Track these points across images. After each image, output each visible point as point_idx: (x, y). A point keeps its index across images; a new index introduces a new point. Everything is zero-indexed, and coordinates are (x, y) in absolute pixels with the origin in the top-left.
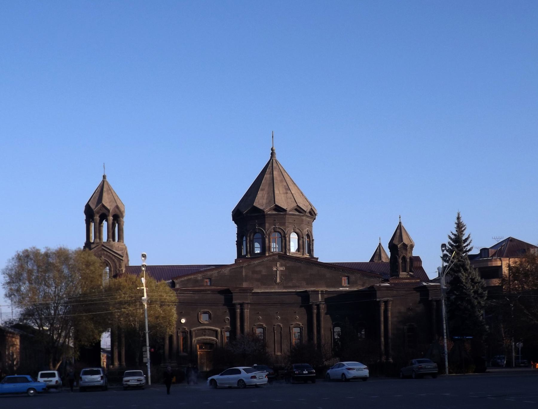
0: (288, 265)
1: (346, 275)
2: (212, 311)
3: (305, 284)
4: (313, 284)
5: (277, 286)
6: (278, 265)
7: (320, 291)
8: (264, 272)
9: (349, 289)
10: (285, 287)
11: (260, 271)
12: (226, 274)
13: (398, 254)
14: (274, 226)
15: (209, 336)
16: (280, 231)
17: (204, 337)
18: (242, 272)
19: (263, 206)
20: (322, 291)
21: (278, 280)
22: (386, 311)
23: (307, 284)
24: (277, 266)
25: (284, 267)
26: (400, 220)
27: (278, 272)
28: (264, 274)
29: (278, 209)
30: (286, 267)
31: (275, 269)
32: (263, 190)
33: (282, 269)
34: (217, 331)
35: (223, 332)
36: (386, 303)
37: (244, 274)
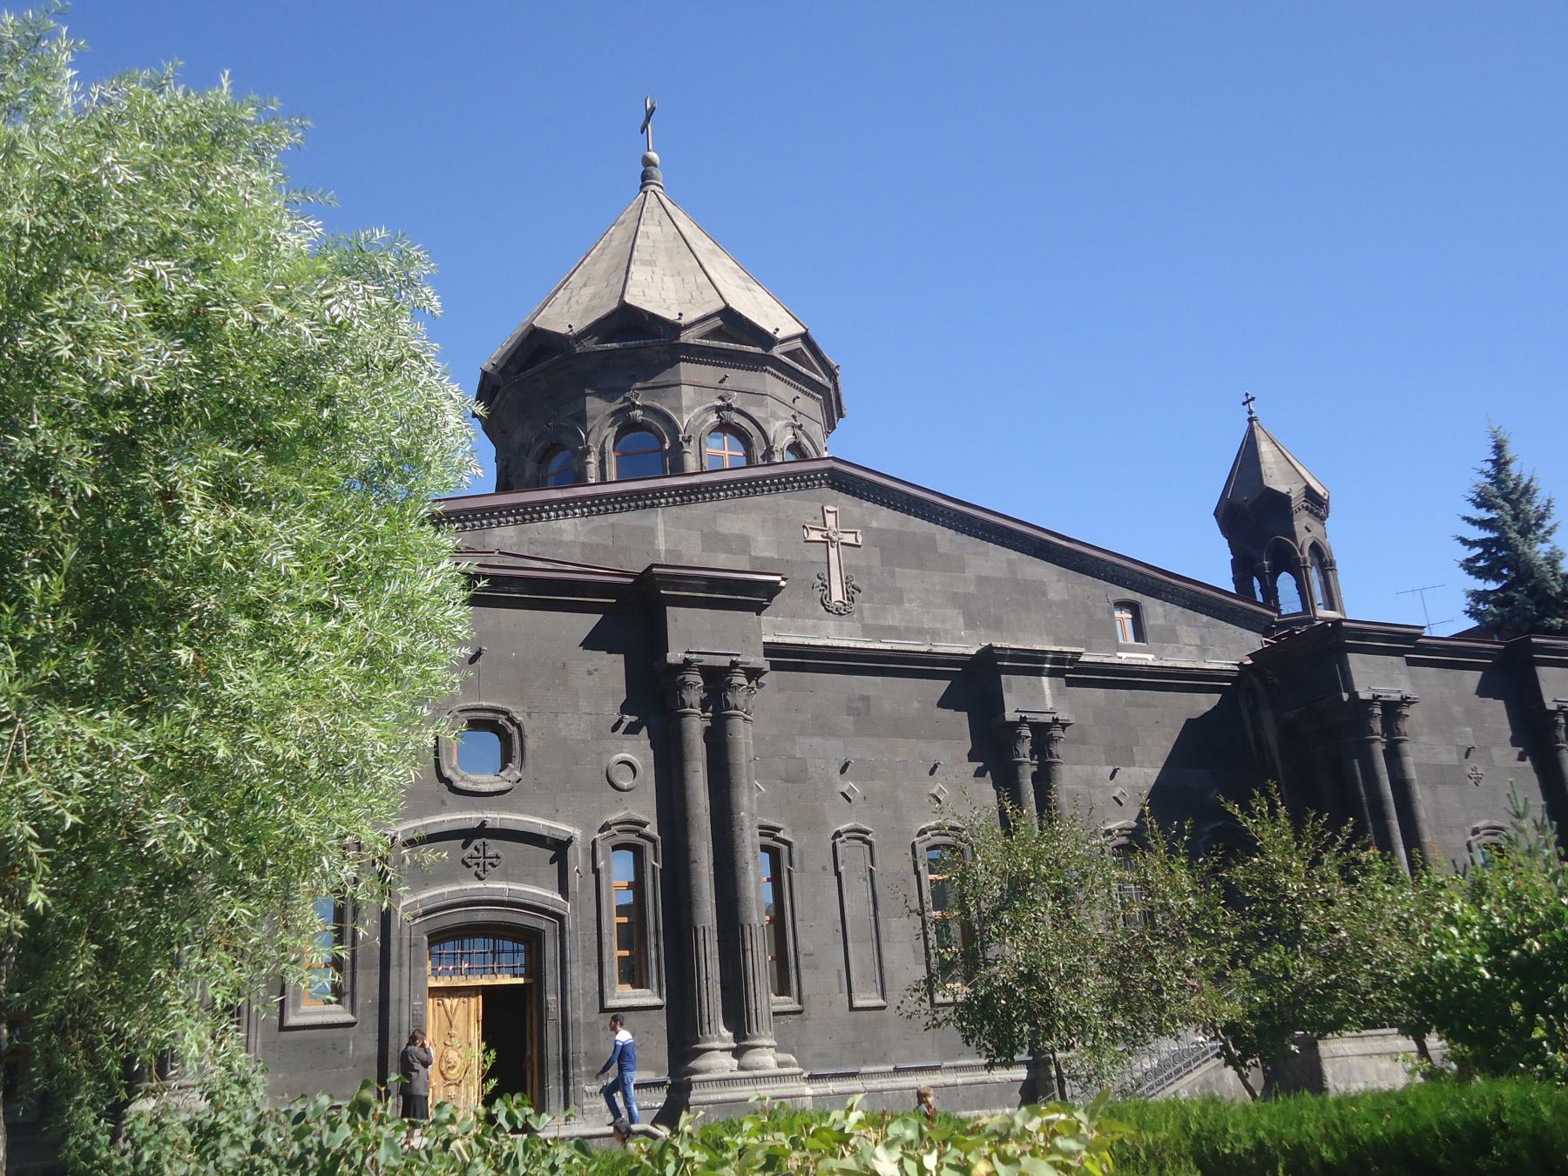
0: (875, 524)
2: (529, 715)
3: (962, 621)
4: (997, 625)
5: (832, 623)
6: (830, 519)
10: (868, 631)
11: (745, 542)
12: (566, 538)
13: (1293, 535)
14: (719, 403)
15: (507, 877)
16: (745, 423)
17: (480, 885)
18: (652, 531)
19: (668, 309)
20: (1059, 658)
21: (837, 594)
22: (1394, 755)
24: (825, 526)
25: (859, 531)
26: (1250, 412)
27: (833, 552)
29: (731, 323)
30: (867, 530)
31: (816, 536)
32: (650, 263)
33: (850, 539)
34: (559, 848)
35: (599, 855)
36: (1393, 710)
37: (661, 544)
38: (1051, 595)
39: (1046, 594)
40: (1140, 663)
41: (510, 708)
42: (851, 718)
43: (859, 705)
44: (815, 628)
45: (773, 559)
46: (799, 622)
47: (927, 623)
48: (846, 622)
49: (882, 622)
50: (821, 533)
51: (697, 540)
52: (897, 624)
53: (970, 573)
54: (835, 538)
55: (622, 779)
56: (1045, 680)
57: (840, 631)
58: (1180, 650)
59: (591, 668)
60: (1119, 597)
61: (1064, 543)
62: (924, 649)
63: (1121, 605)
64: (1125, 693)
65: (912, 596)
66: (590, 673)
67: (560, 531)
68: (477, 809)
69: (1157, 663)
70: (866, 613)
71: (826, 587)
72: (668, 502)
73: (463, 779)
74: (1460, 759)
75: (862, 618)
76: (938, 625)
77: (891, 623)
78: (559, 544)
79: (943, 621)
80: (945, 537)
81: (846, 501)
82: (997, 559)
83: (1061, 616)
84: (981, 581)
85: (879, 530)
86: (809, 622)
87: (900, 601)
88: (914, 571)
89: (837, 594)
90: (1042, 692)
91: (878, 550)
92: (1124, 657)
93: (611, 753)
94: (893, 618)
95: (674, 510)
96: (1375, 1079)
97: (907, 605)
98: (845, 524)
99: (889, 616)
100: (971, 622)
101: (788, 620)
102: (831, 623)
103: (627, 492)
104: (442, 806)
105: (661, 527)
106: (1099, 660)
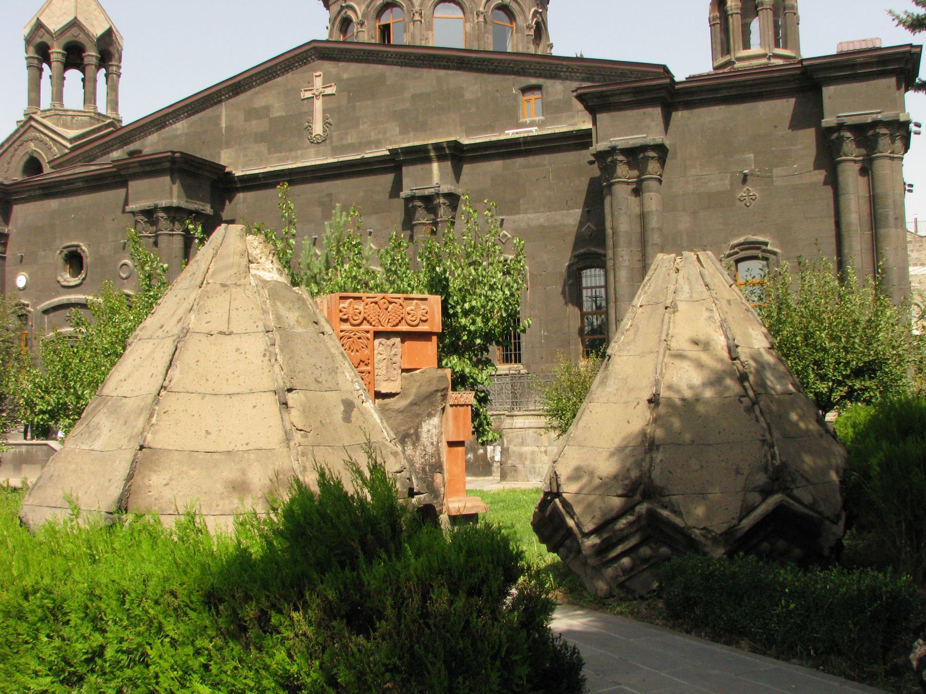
0: (345, 76)
1: (533, 81)
3: (397, 129)
4: (422, 127)
6: (318, 83)
7: (430, 147)
8: (278, 112)
9: (536, 131)
10: (335, 151)
11: (267, 108)
12: (179, 132)
20: (438, 147)
21: (318, 129)
23: (404, 131)
27: (318, 104)
28: (278, 114)
30: (338, 81)
31: (308, 95)
33: (329, 91)
37: (223, 125)
38: (468, 96)
39: (462, 96)
40: (522, 135)
41: (81, 244)
42: (320, 209)
43: (326, 199)
44: (303, 156)
45: (282, 117)
46: (293, 154)
47: (373, 136)
48: (322, 148)
49: (345, 142)
50: (310, 92)
51: (241, 116)
52: (354, 141)
53: (407, 95)
54: (317, 93)
55: (124, 273)
56: (435, 166)
57: (317, 154)
58: (573, 117)
59: (114, 217)
60: (523, 85)
61: (474, 55)
62: (359, 157)
63: (525, 90)
64: (520, 161)
65: (365, 120)
66: (113, 220)
67: (177, 129)
68: (70, 294)
69: (540, 133)
70: (334, 139)
71: (309, 129)
72: (226, 98)
73: (65, 281)
74: (732, 184)
75: (332, 142)
76: (381, 136)
77: (350, 141)
78: (176, 137)
79: (385, 133)
80: (391, 73)
81: (329, 65)
82: (429, 77)
83: (474, 110)
84: (415, 97)
85: (348, 79)
86: (299, 152)
87: (358, 125)
88: (369, 102)
89: (318, 129)
90: (430, 172)
91: (346, 93)
92: (510, 134)
93: (120, 260)
94: (351, 139)
95: (230, 101)
96: (546, 444)
97: (361, 127)
98: (326, 83)
99: (349, 137)
100: (404, 131)
101: (287, 154)
102: (312, 150)
103: (192, 103)
104: (58, 294)
105: (224, 113)
106: (487, 140)
